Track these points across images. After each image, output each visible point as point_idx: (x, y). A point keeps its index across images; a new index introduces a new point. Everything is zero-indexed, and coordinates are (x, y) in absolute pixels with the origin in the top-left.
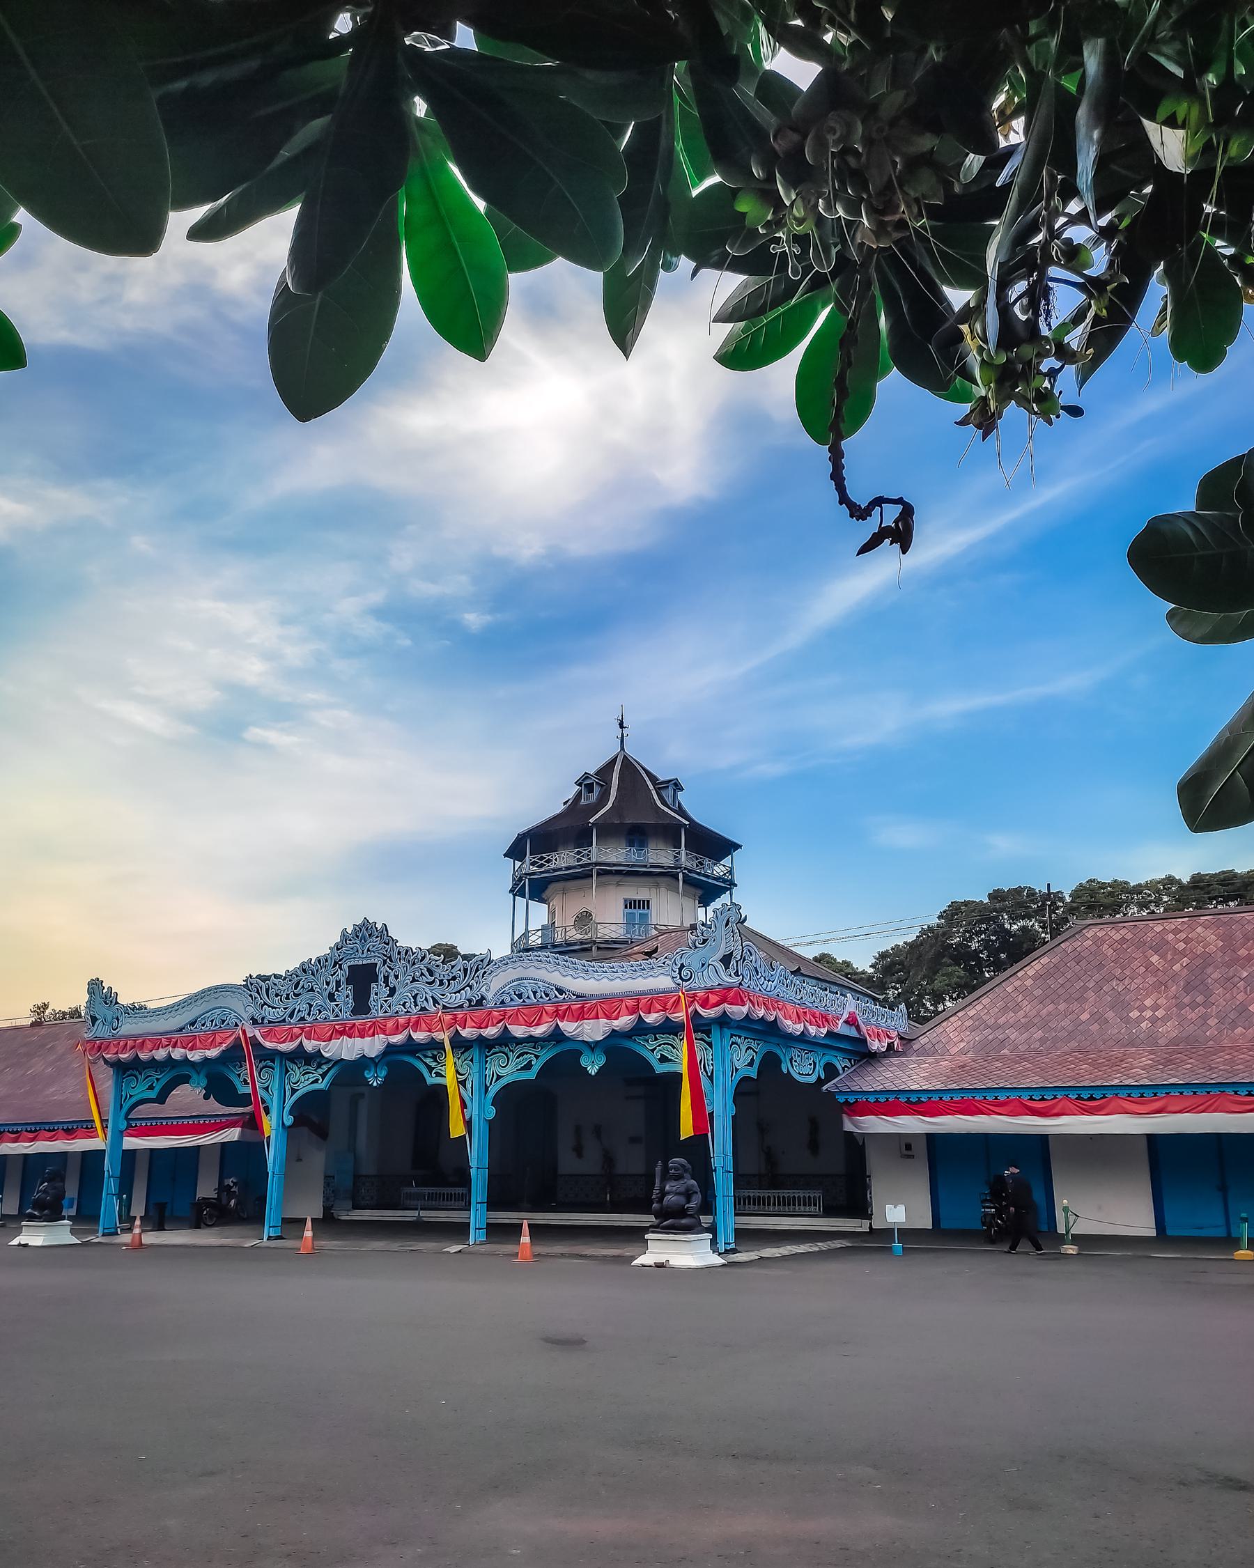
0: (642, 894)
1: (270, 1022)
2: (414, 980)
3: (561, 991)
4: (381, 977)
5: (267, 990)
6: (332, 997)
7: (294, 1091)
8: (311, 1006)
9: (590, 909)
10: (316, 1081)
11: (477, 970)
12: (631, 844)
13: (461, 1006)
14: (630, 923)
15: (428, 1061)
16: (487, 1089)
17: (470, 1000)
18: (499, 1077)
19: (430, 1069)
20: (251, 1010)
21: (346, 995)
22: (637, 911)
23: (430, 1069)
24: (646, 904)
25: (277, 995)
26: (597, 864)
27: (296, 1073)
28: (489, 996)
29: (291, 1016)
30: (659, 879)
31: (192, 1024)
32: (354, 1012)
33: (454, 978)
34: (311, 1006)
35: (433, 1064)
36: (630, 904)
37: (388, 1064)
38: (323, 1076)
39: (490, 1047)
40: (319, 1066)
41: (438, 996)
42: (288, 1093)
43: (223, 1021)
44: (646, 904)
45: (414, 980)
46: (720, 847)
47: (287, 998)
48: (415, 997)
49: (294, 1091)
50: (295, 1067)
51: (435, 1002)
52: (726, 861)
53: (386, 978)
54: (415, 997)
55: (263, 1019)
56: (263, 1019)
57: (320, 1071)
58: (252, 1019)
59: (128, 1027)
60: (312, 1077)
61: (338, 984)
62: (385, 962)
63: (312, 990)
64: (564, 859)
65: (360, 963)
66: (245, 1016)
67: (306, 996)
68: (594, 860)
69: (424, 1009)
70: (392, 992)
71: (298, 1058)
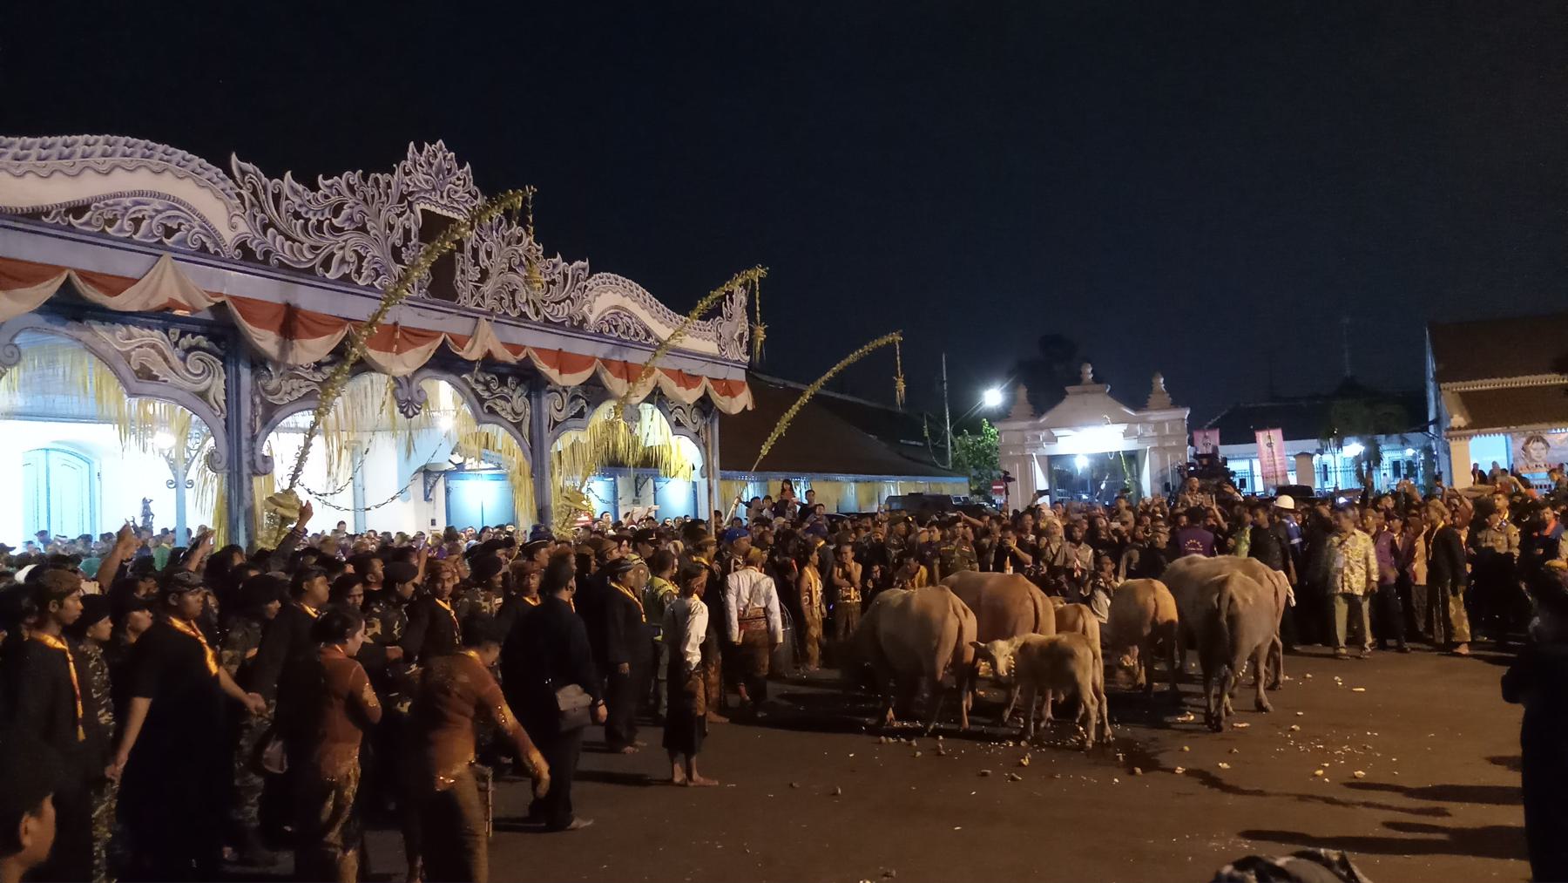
3: (649, 334)
5: (277, 198)
8: (361, 258)
15: (479, 388)
20: (243, 227)
25: (297, 215)
28: (592, 318)
29: (326, 264)
31: (78, 210)
34: (361, 258)
35: (486, 395)
43: (169, 232)
47: (319, 227)
53: (475, 252)
55: (267, 254)
56: (267, 254)
58: (242, 246)
61: (407, 232)
66: (229, 237)
69: (523, 315)
70: (485, 274)
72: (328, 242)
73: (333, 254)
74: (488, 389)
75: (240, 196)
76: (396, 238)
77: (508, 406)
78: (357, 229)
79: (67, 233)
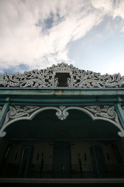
1: (10, 86)
2: (88, 78)
4: (72, 77)
6: (46, 81)
8: (35, 83)
10: (26, 116)
11: (117, 78)
13: (115, 87)
15: (92, 110)
17: (118, 86)
19: (94, 114)
25: (17, 78)
29: (24, 85)
32: (58, 86)
33: (107, 79)
34: (35, 83)
35: (95, 111)
37: (68, 111)
38: (30, 114)
40: (29, 109)
41: (101, 83)
42: (7, 120)
45: (88, 78)
48: (91, 83)
49: (10, 119)
50: (14, 109)
51: (102, 85)
53: (75, 78)
54: (91, 83)
57: (28, 111)
60: (23, 114)
61: (50, 77)
62: (73, 73)
63: (37, 78)
65: (61, 72)
70: (79, 81)
71: (16, 105)
73: (26, 83)
74: (96, 110)
75: (4, 78)
76: (48, 78)
77: (106, 114)
78: (35, 78)
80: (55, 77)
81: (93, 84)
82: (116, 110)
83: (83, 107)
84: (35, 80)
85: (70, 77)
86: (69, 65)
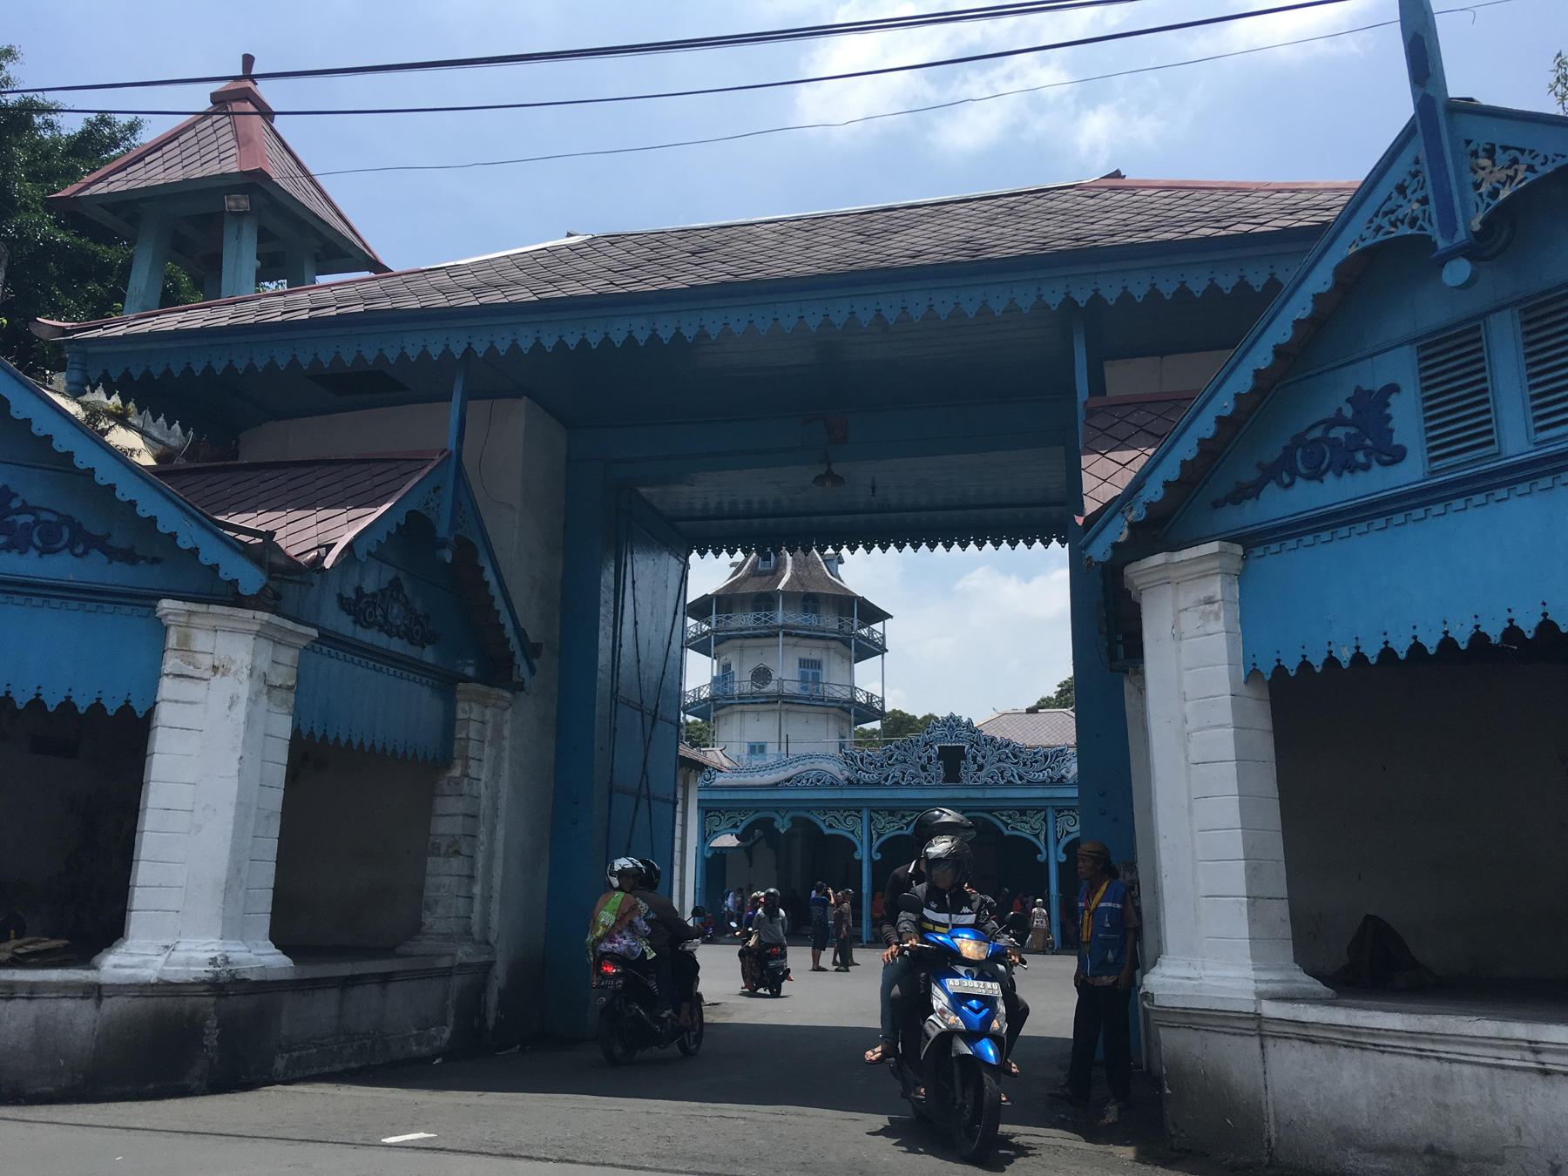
0: (815, 655)
6: (924, 768)
7: (880, 835)
9: (768, 664)
12: (806, 610)
14: (804, 679)
16: (1058, 841)
18: (1068, 833)
19: (1006, 825)
21: (937, 769)
22: (810, 671)
23: (1006, 825)
24: (817, 665)
26: (782, 627)
27: (881, 821)
29: (886, 779)
30: (833, 644)
31: (788, 780)
36: (803, 663)
38: (908, 825)
39: (1059, 811)
40: (903, 817)
41: (1022, 772)
44: (817, 665)
46: (873, 614)
49: (880, 835)
51: (1021, 778)
52: (877, 626)
53: (974, 759)
59: (720, 780)
61: (930, 759)
64: (744, 620)
67: (898, 767)
68: (780, 622)
70: (981, 768)
72: (886, 770)
79: (787, 789)
80: (939, 758)
81: (1007, 774)
82: (1045, 820)
83: (990, 811)
84: (904, 766)
85: (965, 758)
86: (965, 720)
